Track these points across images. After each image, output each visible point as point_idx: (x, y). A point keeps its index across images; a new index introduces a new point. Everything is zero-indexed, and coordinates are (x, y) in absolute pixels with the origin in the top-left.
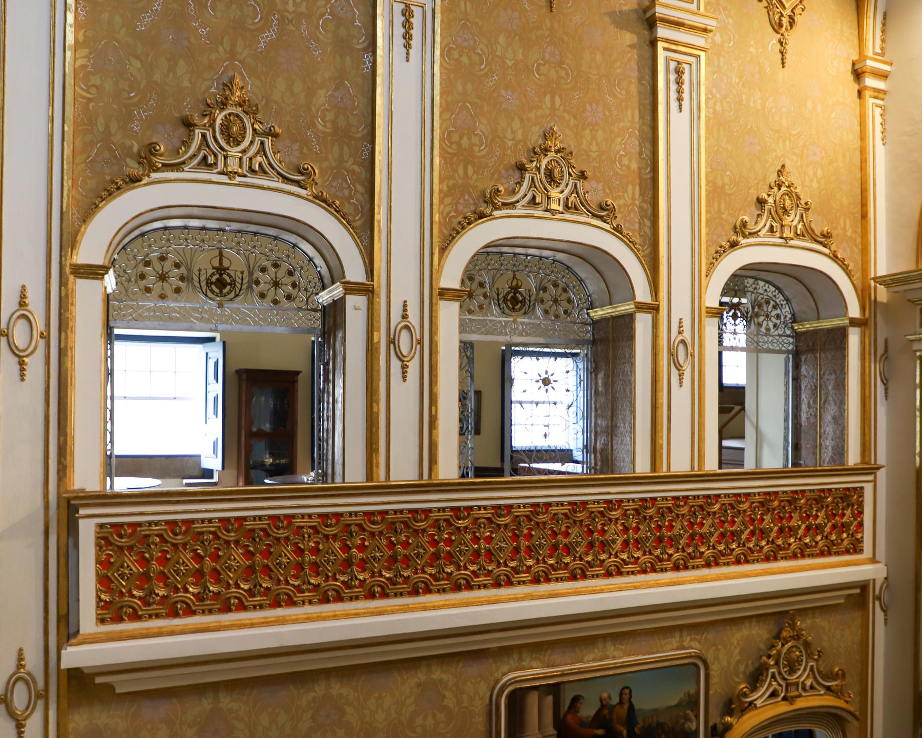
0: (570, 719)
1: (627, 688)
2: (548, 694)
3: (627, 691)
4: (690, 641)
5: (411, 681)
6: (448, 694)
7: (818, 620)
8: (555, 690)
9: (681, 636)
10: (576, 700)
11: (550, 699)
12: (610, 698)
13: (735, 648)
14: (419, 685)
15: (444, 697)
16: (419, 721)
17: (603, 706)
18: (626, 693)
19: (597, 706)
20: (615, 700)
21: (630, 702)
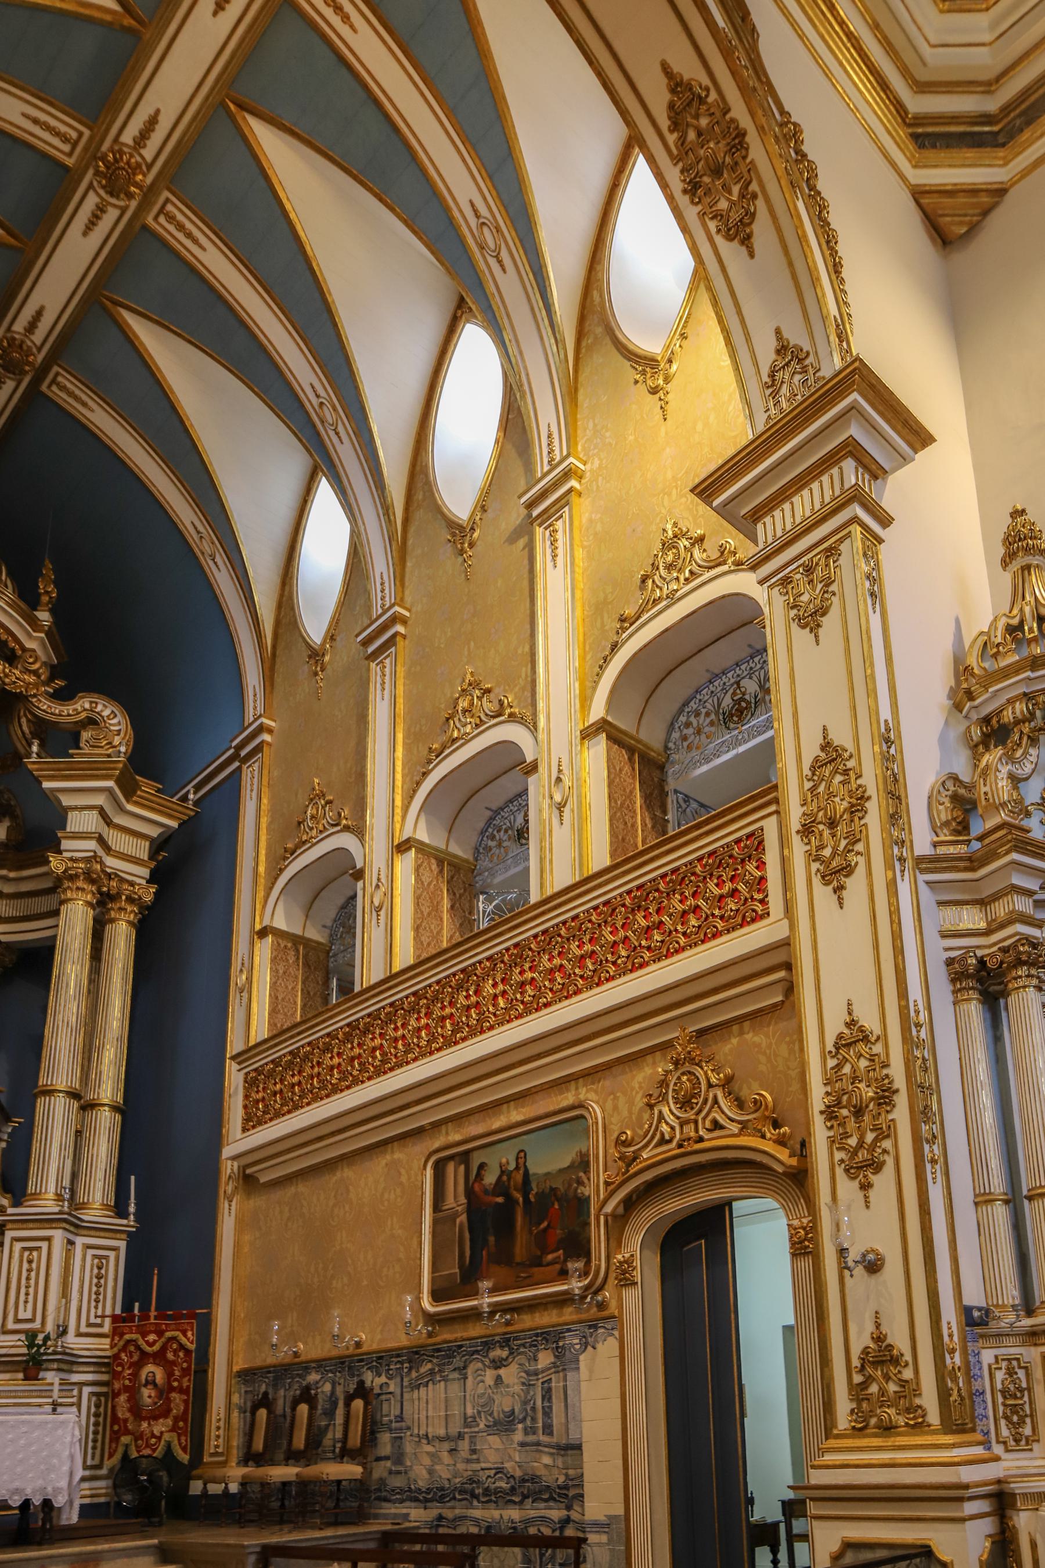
0: (477, 1187)
1: (522, 1151)
2: (460, 1164)
3: (522, 1154)
4: (587, 1091)
5: (380, 1164)
6: (403, 1171)
7: (749, 1036)
8: (464, 1157)
9: (577, 1089)
10: (482, 1166)
11: (462, 1168)
12: (508, 1163)
13: (637, 1093)
14: (387, 1164)
15: (400, 1174)
16: (386, 1196)
17: (503, 1172)
18: (521, 1156)
19: (498, 1173)
20: (512, 1166)
21: (525, 1166)
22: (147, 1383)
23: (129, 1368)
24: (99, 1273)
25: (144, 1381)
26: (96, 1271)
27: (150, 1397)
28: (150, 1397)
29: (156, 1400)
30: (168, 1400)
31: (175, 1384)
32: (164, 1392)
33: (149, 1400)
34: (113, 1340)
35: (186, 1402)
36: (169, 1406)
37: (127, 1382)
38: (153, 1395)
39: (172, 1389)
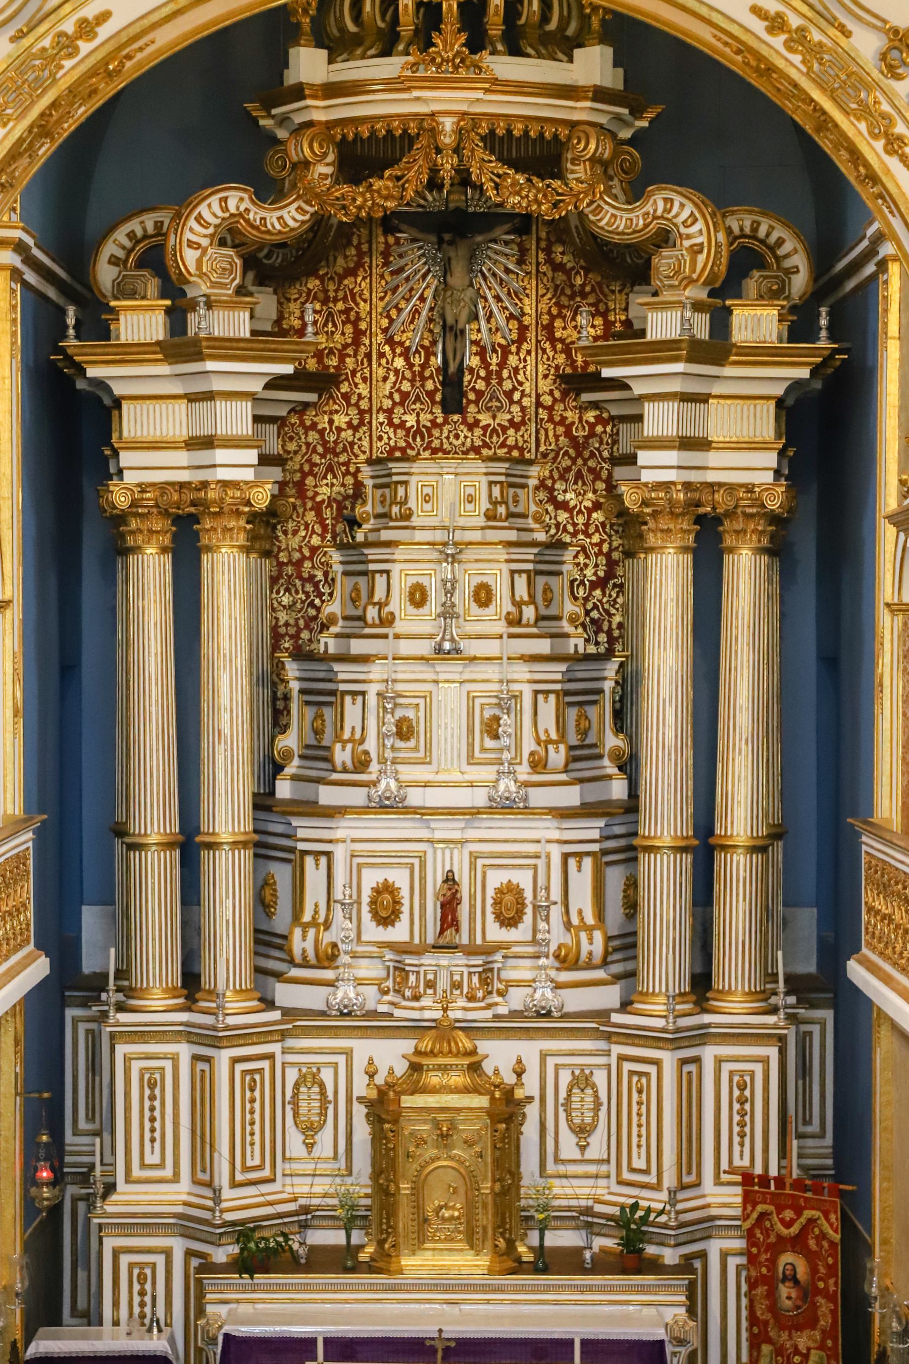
22: (785, 1279)
23: (766, 1251)
24: (742, 1094)
25: (781, 1276)
26: (736, 1093)
27: (789, 1298)
28: (789, 1298)
29: (799, 1303)
30: (814, 1307)
31: (821, 1285)
32: (808, 1293)
33: (788, 1304)
34: (745, 1209)
35: (833, 1312)
36: (815, 1313)
37: (764, 1270)
38: (793, 1295)
39: (817, 1292)
